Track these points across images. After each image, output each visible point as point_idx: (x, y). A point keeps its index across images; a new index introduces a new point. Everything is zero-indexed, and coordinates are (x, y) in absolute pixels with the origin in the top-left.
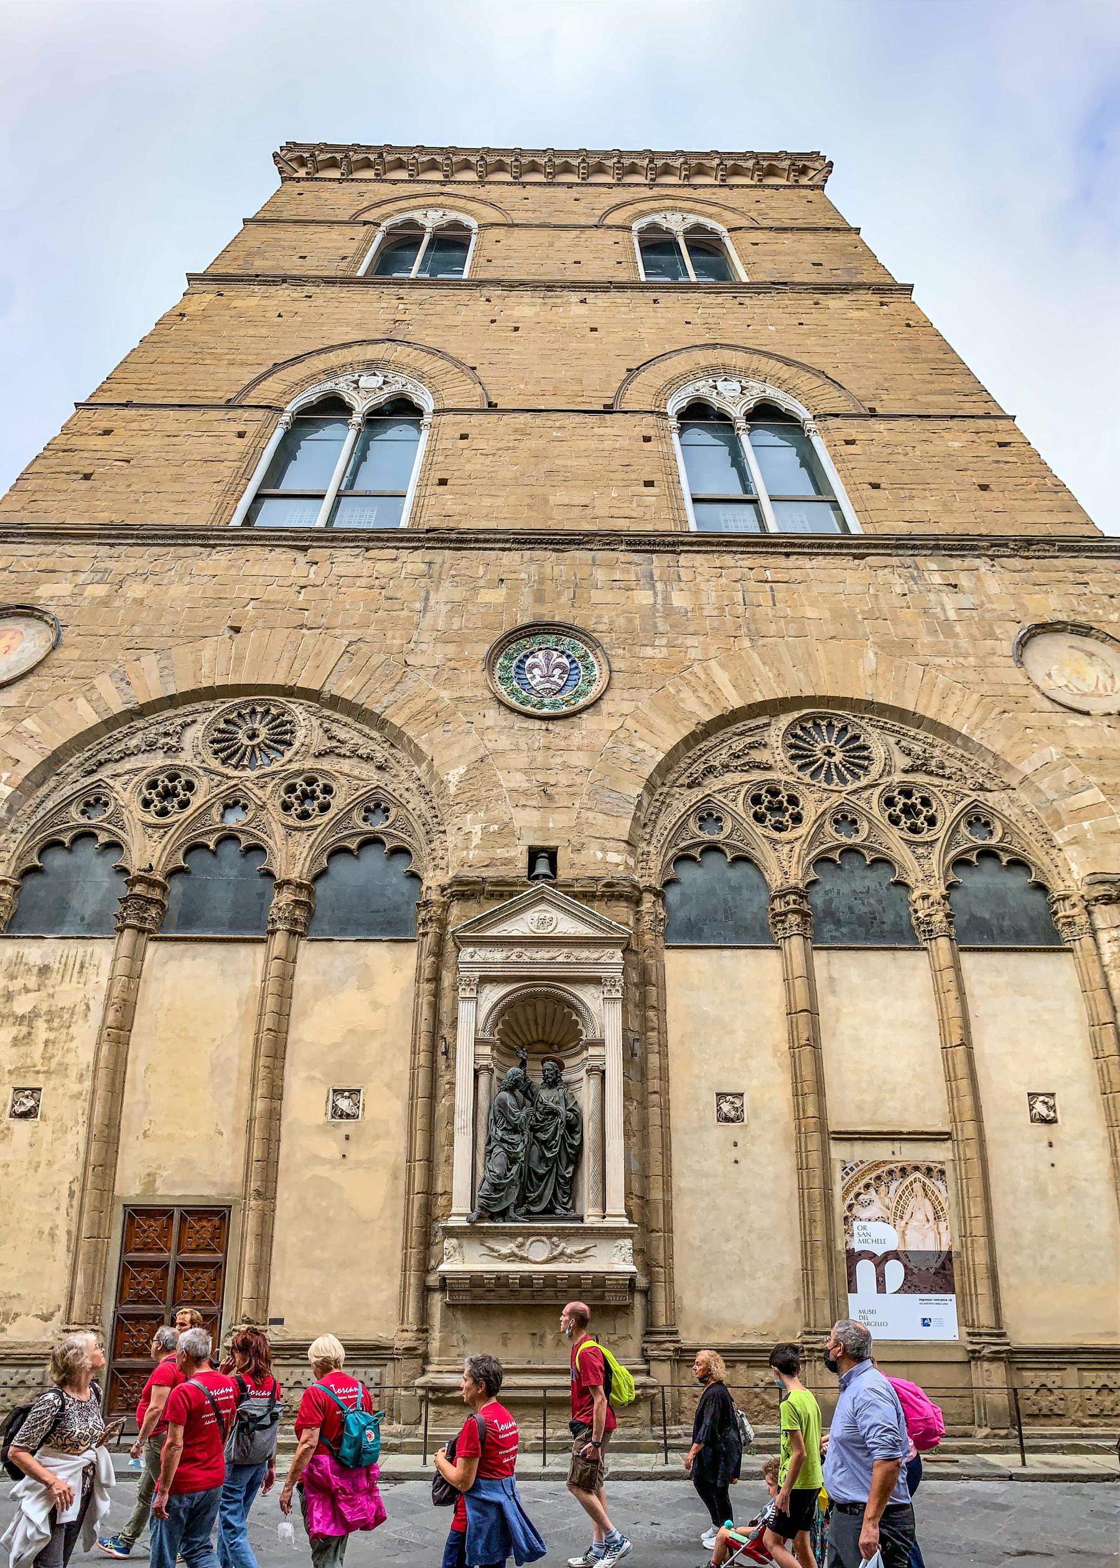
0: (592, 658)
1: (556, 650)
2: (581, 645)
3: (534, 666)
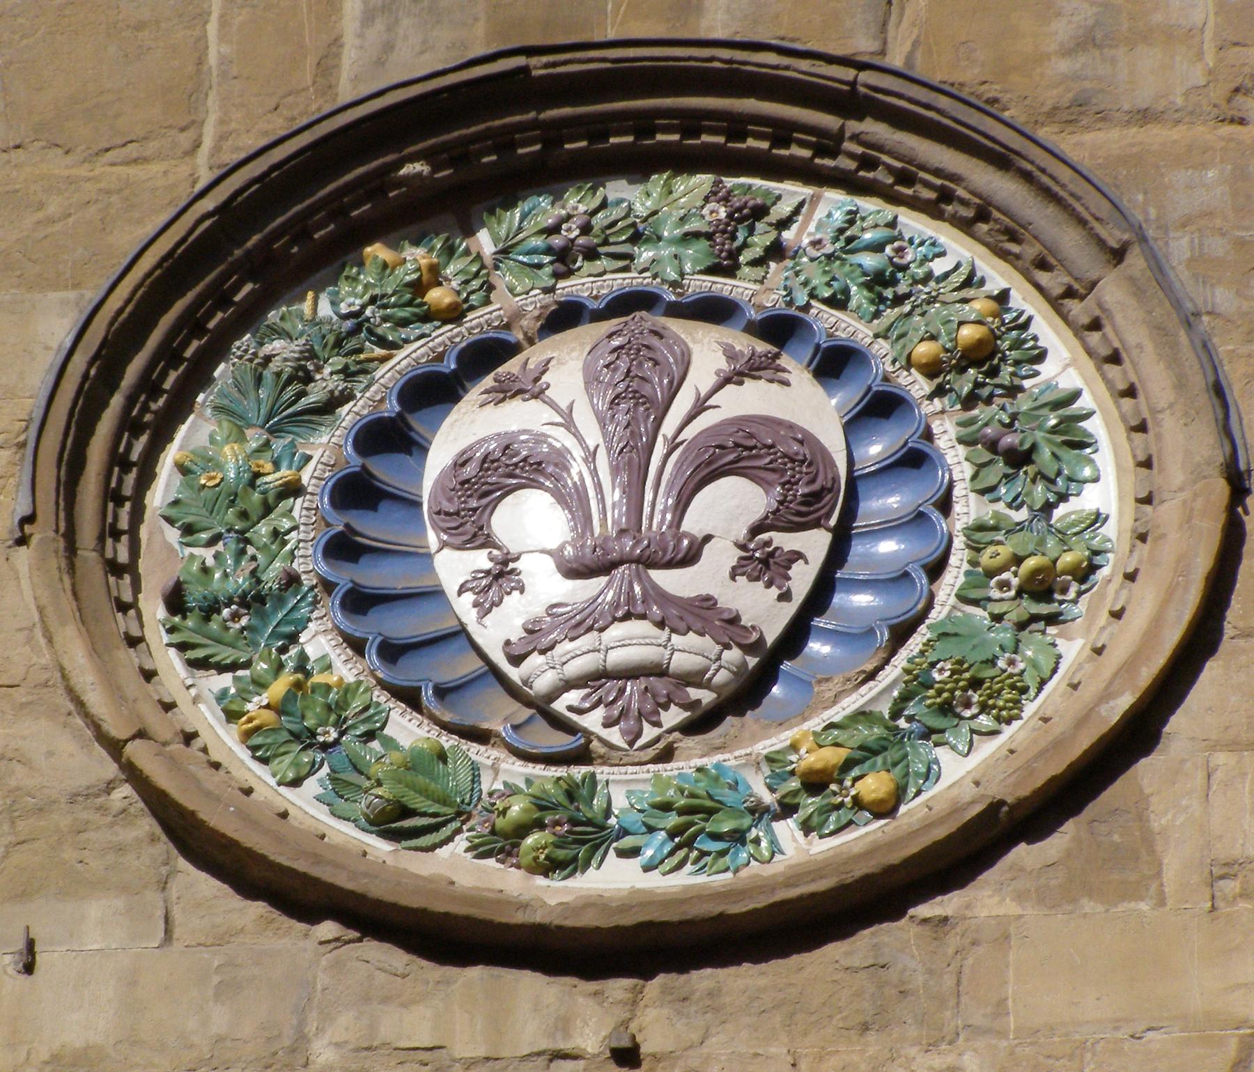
0: (1062, 366)
1: (714, 311)
2: (958, 250)
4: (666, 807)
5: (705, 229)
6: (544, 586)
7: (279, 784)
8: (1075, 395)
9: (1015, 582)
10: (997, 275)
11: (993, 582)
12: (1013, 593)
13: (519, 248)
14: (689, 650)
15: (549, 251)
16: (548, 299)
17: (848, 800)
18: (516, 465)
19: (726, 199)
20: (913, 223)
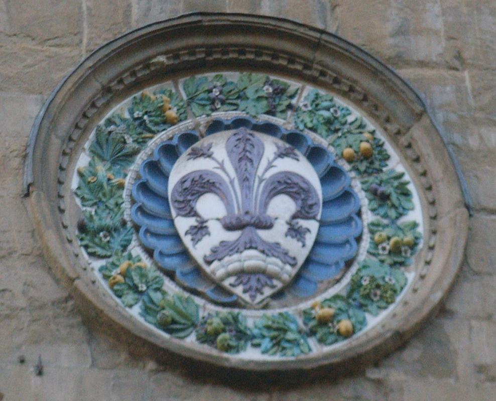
0: (396, 164)
1: (270, 129)
2: (355, 114)
3: (201, 185)
4: (268, 328)
5: (265, 95)
6: (217, 235)
7: (126, 306)
8: (402, 175)
9: (388, 247)
10: (371, 125)
11: (380, 247)
12: (386, 252)
13: (197, 98)
14: (273, 264)
15: (209, 99)
16: (209, 119)
17: (335, 331)
18: (205, 183)
19: (271, 85)
20: (340, 101)
